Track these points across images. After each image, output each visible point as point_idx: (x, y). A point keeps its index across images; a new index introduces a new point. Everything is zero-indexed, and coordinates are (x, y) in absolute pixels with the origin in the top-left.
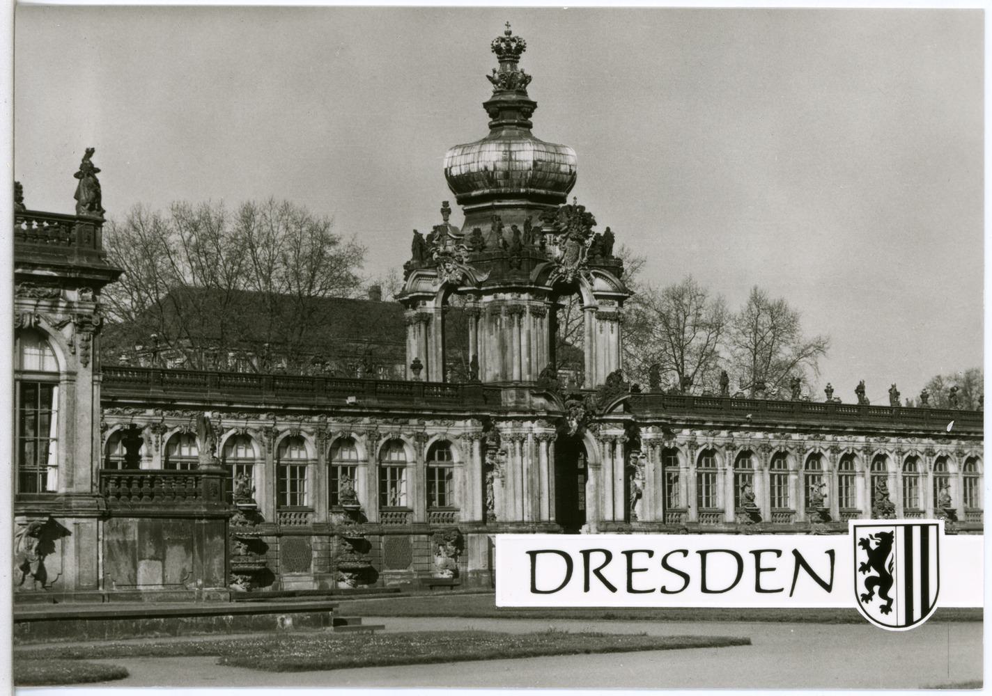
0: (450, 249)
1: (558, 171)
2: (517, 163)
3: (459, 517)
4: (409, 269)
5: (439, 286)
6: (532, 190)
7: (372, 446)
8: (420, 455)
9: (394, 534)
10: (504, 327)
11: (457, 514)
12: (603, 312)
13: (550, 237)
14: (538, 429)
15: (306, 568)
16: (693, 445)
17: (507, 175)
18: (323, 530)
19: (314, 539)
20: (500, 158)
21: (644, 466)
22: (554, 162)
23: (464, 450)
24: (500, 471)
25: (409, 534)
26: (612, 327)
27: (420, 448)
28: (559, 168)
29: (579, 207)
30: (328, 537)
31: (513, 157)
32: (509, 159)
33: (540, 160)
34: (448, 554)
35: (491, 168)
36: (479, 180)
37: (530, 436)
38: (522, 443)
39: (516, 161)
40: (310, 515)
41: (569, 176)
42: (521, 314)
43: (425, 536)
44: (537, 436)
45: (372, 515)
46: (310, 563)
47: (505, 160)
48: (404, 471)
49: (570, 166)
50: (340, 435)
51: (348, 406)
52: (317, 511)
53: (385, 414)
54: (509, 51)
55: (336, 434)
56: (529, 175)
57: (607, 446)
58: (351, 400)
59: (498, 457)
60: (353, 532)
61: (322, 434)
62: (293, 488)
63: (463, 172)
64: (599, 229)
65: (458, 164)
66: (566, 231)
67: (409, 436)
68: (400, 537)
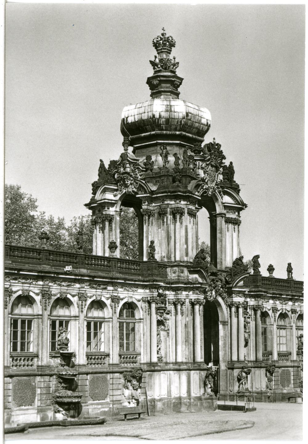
0: (128, 170)
1: (199, 122)
2: (175, 114)
3: (140, 359)
4: (96, 187)
5: (119, 196)
6: (184, 133)
7: (82, 305)
8: (115, 313)
9: (96, 373)
10: (169, 222)
11: (138, 358)
12: (229, 218)
13: (199, 163)
14: (193, 296)
15: (31, 403)
16: (275, 310)
17: (168, 120)
18: (43, 372)
19: (38, 379)
20: (164, 110)
21: (250, 323)
22: (198, 116)
23: (144, 310)
24: (166, 326)
25: (107, 373)
26: (234, 228)
27: (115, 307)
28: (200, 120)
29: (217, 144)
30: (48, 377)
31: (173, 109)
32: (169, 109)
33: (191, 113)
34: (133, 387)
35: (157, 116)
36: (148, 125)
37: (187, 301)
38: (182, 305)
39: (174, 112)
40: (36, 359)
41: (206, 127)
42: (182, 214)
43: (118, 374)
44: (193, 301)
45: (80, 359)
46: (35, 398)
47: (167, 111)
48: (103, 325)
49: (207, 120)
50: (59, 296)
51: (66, 273)
52: (40, 357)
53: (93, 282)
54: (164, 44)
55: (55, 295)
56: (183, 122)
57: (233, 309)
58: (68, 268)
59: (165, 315)
60: (66, 371)
61: (46, 294)
62: (23, 338)
63: (136, 120)
64: (227, 163)
65: (133, 115)
66: (209, 160)
67: (108, 299)
68: (100, 375)
